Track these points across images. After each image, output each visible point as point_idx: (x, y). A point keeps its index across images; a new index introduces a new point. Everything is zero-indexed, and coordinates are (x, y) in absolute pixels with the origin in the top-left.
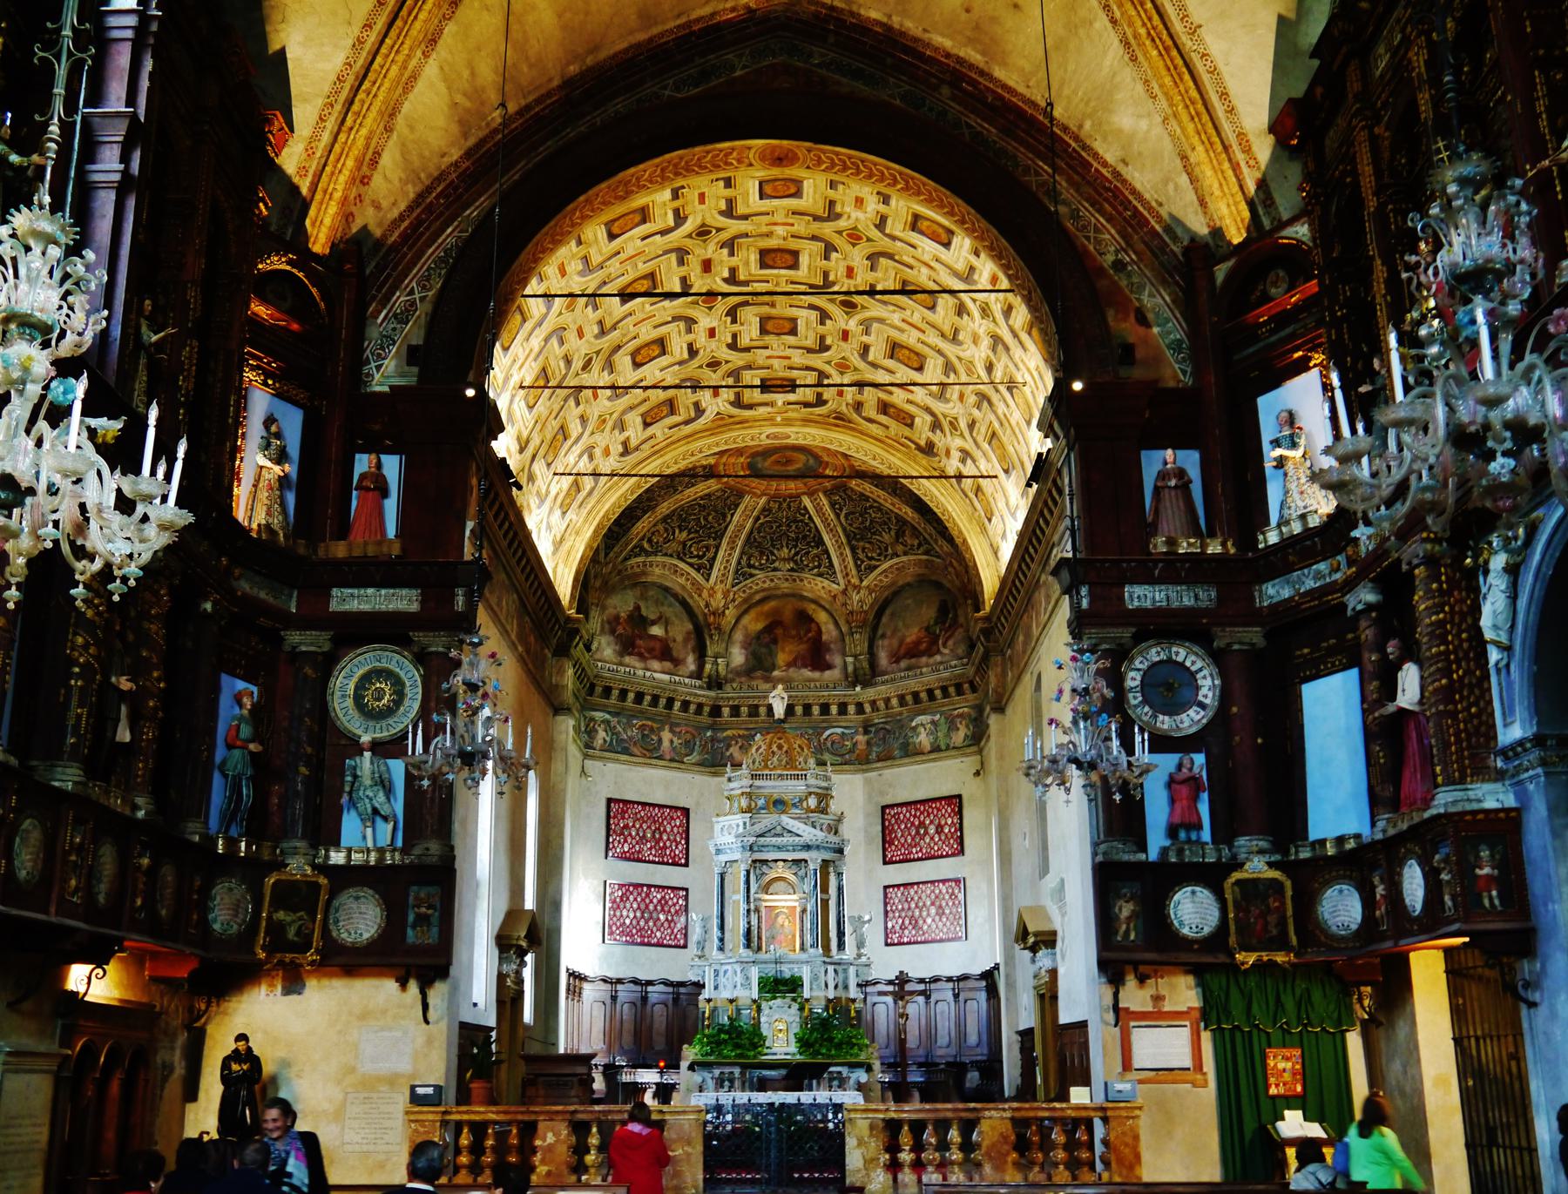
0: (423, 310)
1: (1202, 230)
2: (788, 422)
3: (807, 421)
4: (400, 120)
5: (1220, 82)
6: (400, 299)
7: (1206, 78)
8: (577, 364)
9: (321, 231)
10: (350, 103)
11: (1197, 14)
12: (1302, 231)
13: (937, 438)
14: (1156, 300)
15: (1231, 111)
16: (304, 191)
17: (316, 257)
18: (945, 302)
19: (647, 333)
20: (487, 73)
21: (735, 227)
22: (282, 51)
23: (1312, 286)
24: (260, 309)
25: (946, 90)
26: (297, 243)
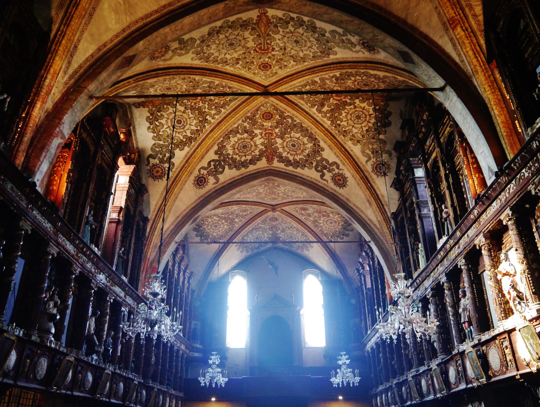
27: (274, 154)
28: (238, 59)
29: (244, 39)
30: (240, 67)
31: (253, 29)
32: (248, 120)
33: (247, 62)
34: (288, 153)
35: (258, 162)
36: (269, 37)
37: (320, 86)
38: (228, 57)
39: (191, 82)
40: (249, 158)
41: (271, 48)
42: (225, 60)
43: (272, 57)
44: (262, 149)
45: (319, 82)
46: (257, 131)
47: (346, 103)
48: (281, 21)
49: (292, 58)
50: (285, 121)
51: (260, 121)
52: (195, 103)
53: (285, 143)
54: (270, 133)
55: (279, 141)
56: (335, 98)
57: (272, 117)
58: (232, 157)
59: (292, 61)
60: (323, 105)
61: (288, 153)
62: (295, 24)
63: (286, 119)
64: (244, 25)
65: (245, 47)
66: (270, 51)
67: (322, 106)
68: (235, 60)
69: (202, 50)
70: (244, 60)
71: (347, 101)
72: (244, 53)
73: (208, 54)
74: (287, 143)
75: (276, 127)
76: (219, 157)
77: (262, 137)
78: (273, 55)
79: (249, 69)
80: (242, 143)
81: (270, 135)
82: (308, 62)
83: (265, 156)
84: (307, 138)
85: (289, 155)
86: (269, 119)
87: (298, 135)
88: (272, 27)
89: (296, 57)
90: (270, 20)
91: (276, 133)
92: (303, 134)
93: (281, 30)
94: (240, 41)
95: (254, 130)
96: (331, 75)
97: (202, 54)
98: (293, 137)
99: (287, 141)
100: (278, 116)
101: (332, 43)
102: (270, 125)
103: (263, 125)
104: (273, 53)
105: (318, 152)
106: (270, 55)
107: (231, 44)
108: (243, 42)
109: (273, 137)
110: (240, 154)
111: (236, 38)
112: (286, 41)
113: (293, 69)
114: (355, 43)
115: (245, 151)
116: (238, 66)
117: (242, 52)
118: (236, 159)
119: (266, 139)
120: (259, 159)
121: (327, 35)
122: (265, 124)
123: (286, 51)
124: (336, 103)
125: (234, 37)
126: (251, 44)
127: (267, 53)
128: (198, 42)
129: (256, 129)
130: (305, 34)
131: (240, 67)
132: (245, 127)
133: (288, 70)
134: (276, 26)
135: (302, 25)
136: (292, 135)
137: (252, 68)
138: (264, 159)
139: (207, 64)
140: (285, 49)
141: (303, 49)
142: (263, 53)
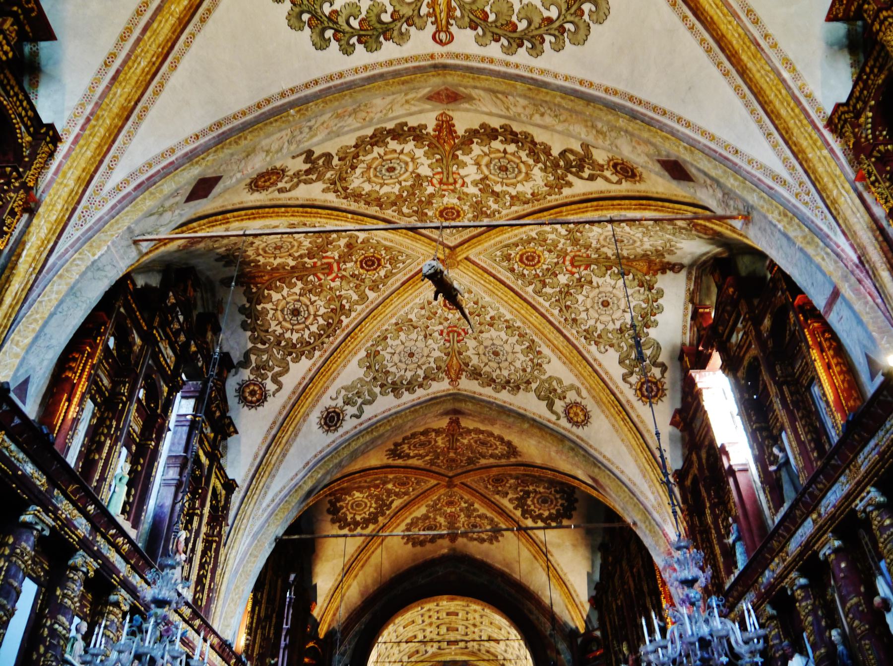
0: (349, 652)
1: (574, 627)
2: (456, 654)
3: (462, 654)
4: (345, 598)
5: (573, 588)
6: (343, 648)
7: (569, 586)
8: (389, 648)
9: (322, 631)
10: (333, 595)
11: (565, 570)
12: (598, 633)
13: (505, 663)
14: (562, 646)
15: (577, 596)
16: (318, 620)
17: (321, 640)
18: (501, 643)
19: (411, 634)
20: (369, 581)
21: (438, 608)
22: (316, 585)
23: (602, 651)
24: (306, 660)
25: (499, 579)
26: (315, 636)
27: (435, 141)
28: (491, 325)
29: (478, 354)
30: (489, 309)
31: (467, 365)
32: (489, 212)
33: (479, 315)
34: (402, 152)
35: (477, 127)
36: (447, 351)
37: (363, 281)
38: (503, 335)
39: (568, 307)
40: (496, 144)
41: (444, 334)
42: (509, 331)
43: (442, 321)
44: (463, 154)
45: (367, 291)
46: (472, 190)
47: (310, 255)
48: (433, 376)
49: (415, 324)
50: (415, 208)
51: (466, 208)
52: (580, 251)
53: (411, 168)
54: (444, 184)
55: (424, 171)
56: (332, 260)
57: (441, 212)
58: (537, 161)
59: (414, 319)
60: (349, 246)
61: (402, 152)
62: (416, 380)
63: (414, 211)
64: (477, 374)
65: (478, 342)
66: (445, 331)
67: (351, 244)
68: (495, 326)
69: (533, 368)
70: (482, 321)
71: (309, 258)
72: (481, 332)
73: (527, 356)
74: (407, 170)
75: (432, 196)
76: (566, 176)
77: (462, 178)
78: (441, 323)
79: (476, 303)
80: (507, 178)
81: (445, 180)
82: (392, 324)
83: (458, 137)
84: (364, 193)
85: (398, 148)
86: (446, 208)
87: (385, 190)
88: (443, 366)
89: (409, 329)
90: (446, 375)
91: (433, 185)
92: (374, 196)
93: (433, 365)
94: (484, 354)
95: (479, 193)
96: (353, 314)
97: (535, 361)
98: (394, 184)
99: (408, 174)
100: (430, 213)
101: (368, 380)
102: (445, 200)
103: (459, 199)
104: (441, 327)
105: (334, 183)
106: (446, 324)
107: (496, 354)
108: (481, 352)
109: (438, 177)
110: (517, 161)
111: (489, 361)
112: (425, 349)
113: (411, 305)
114: (346, 407)
115: (504, 162)
116: (492, 313)
117: (484, 335)
118: (527, 155)
119: (453, 173)
120: (473, 134)
121: (377, 390)
122: (456, 201)
123: (423, 333)
124: (327, 252)
125: (490, 363)
126: (471, 343)
127: (449, 327)
128: (534, 386)
129: (476, 196)
130: (402, 372)
131: (489, 309)
132: (496, 202)
133: (417, 300)
134: (439, 368)
135: (409, 383)
136: (398, 186)
137: (472, 304)
138: (460, 129)
139: (534, 338)
140: (425, 337)
141: (403, 347)
142: (455, 326)
